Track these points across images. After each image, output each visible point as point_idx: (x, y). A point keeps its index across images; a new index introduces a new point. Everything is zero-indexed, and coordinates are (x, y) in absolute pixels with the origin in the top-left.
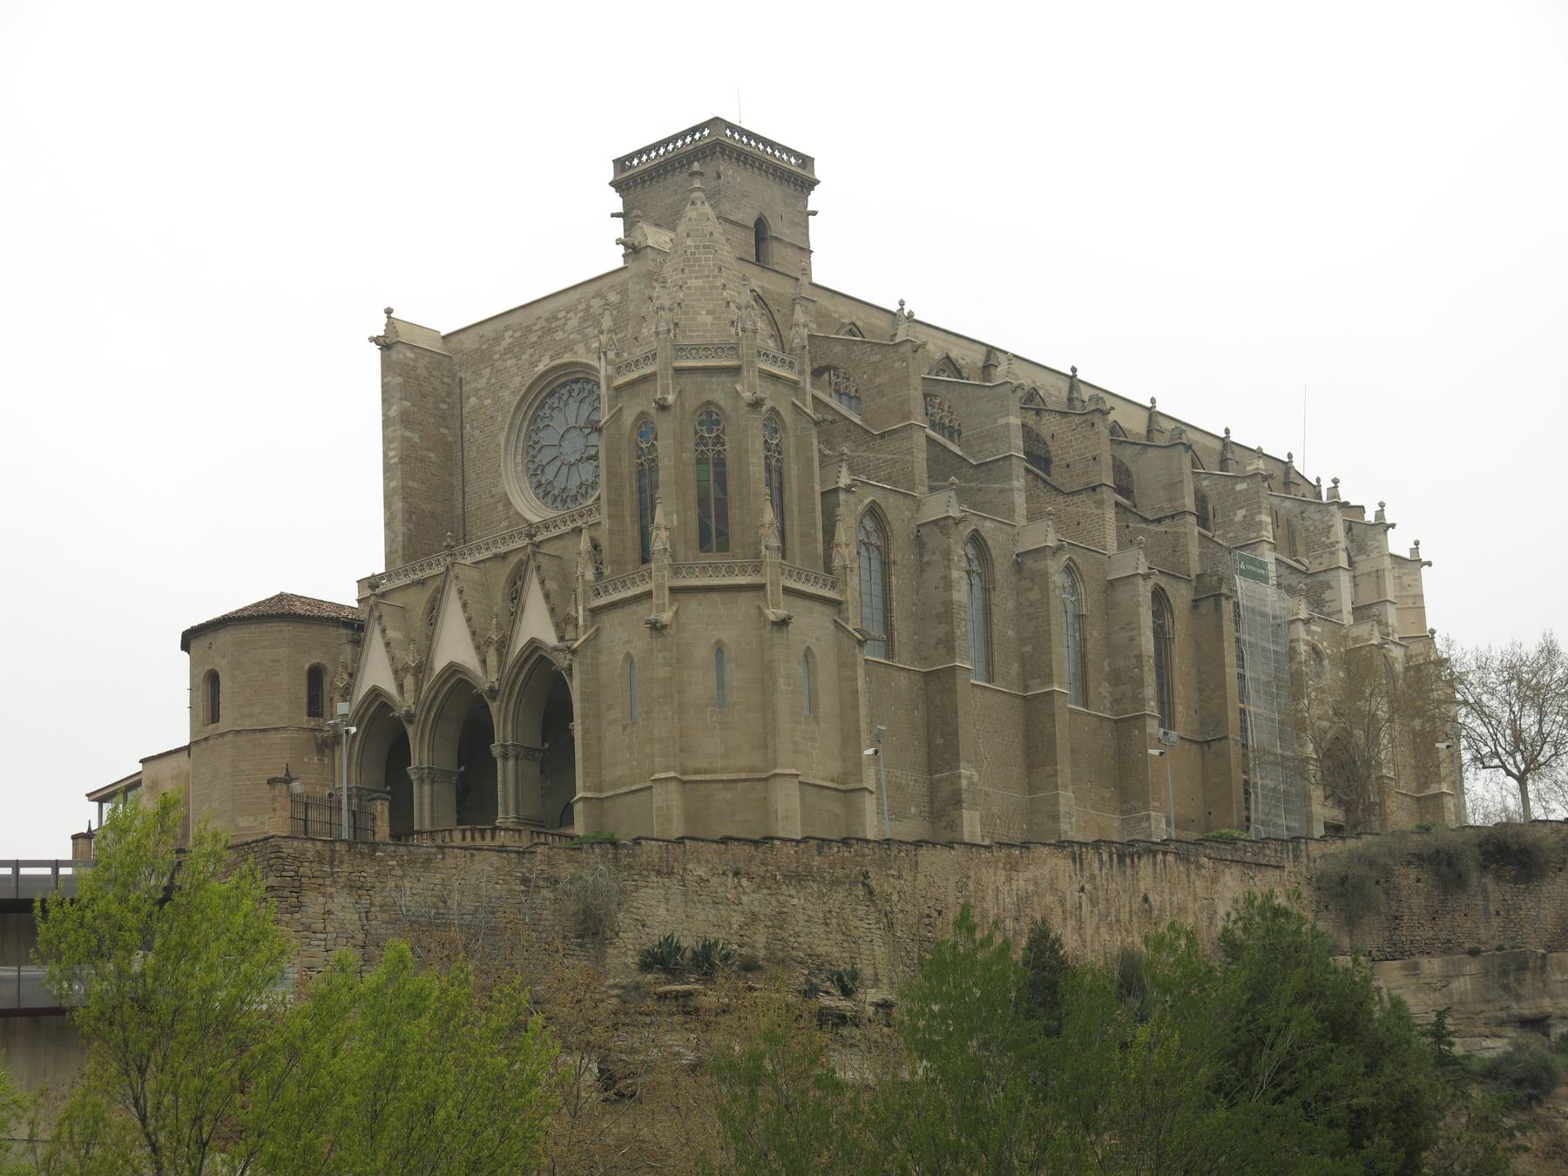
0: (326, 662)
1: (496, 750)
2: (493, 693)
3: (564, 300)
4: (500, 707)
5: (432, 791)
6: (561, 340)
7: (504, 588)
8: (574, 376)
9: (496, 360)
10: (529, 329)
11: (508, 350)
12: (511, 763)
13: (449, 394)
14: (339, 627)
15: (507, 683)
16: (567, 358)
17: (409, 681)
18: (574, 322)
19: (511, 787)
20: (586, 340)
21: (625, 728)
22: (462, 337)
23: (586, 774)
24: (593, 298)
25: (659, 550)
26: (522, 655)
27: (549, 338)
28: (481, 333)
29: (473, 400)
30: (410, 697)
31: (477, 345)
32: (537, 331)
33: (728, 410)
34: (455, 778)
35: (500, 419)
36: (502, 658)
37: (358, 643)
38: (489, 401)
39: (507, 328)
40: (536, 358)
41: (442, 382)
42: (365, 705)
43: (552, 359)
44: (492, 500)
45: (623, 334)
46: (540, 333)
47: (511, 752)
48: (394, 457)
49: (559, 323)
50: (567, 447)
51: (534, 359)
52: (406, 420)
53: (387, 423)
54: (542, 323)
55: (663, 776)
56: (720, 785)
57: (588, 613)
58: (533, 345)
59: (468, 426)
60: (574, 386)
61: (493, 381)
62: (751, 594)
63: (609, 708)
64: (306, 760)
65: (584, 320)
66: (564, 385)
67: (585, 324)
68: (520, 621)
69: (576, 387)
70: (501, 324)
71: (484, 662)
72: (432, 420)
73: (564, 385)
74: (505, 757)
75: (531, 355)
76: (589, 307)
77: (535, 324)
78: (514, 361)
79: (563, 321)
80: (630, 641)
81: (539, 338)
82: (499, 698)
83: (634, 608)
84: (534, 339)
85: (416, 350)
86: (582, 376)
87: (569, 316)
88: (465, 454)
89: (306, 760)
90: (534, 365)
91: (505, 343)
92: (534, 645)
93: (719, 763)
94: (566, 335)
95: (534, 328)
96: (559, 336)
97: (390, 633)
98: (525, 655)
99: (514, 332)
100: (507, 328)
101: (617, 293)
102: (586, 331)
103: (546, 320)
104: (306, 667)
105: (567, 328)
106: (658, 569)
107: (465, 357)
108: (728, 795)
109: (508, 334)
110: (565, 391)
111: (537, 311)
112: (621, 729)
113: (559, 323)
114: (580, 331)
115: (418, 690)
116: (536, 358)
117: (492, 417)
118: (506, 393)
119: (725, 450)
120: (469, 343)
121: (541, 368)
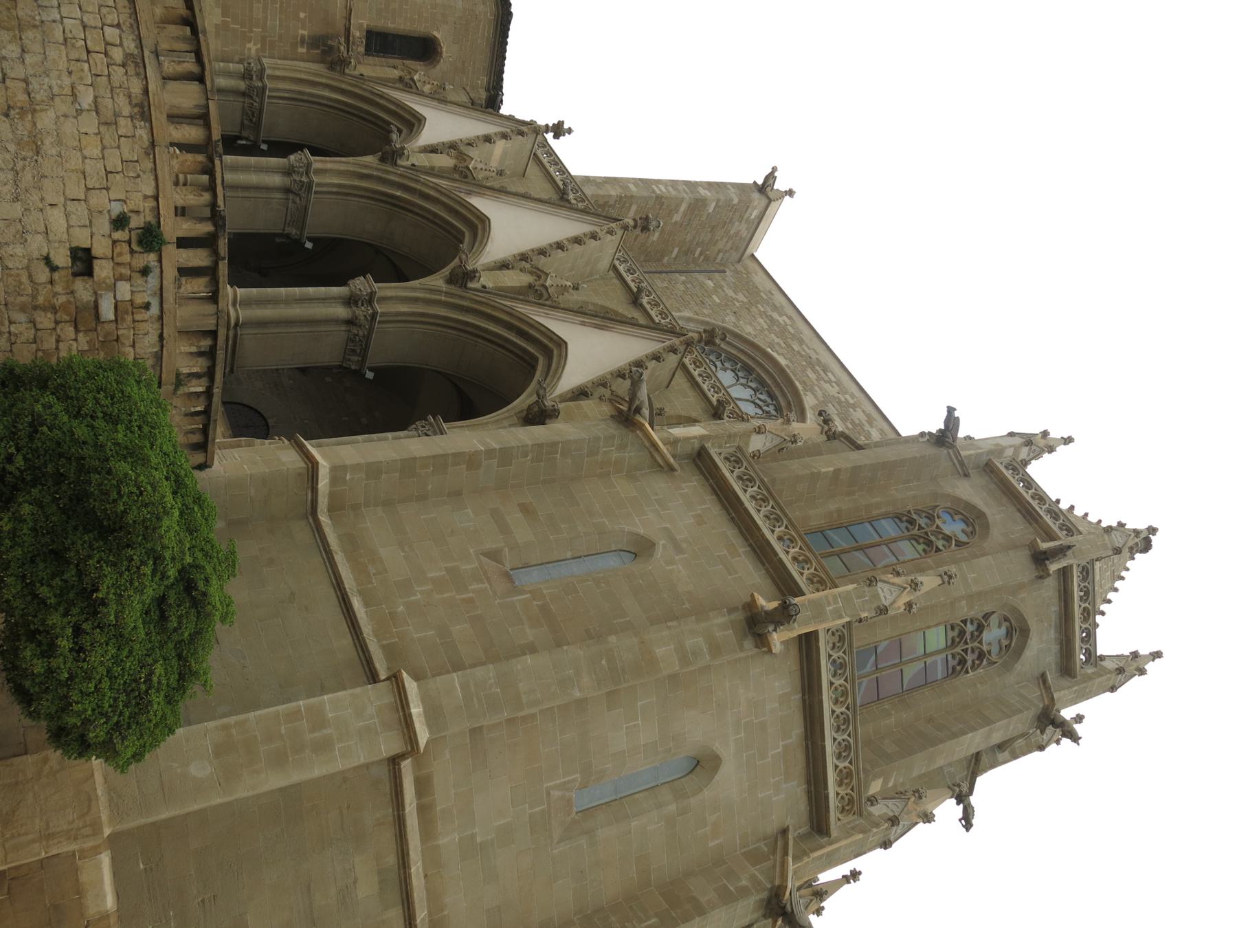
0: (443, 66)
1: (361, 284)
2: (462, 278)
3: (844, 377)
4: (439, 292)
5: (268, 189)
6: (807, 376)
7: (594, 304)
8: (778, 393)
10: (801, 342)
12: (341, 312)
13: (707, 259)
14: (488, 90)
15: (480, 303)
17: (444, 161)
19: (296, 311)
21: (494, 555)
22: (761, 273)
23: (373, 471)
24: (863, 411)
25: (876, 596)
26: (532, 326)
29: (710, 284)
30: (422, 160)
31: (762, 289)
32: (804, 350)
33: (1018, 666)
34: (293, 231)
36: (520, 294)
37: (473, 105)
39: (790, 318)
41: (719, 251)
42: (393, 107)
43: (787, 365)
46: (803, 353)
47: (361, 312)
48: (660, 190)
49: (822, 373)
51: (777, 348)
52: (698, 204)
53: (691, 185)
54: (814, 356)
55: (416, 710)
56: (391, 860)
57: (697, 445)
58: (789, 346)
61: (736, 303)
62: (803, 806)
63: (526, 510)
64: (302, 15)
68: (583, 324)
70: (790, 311)
71: (504, 266)
72: (689, 238)
74: (351, 301)
75: (778, 344)
76: (854, 406)
77: (809, 348)
79: (826, 378)
80: (678, 549)
81: (798, 352)
82: (454, 289)
83: (742, 548)
84: (796, 347)
85: (757, 221)
86: (783, 403)
87: (834, 384)
89: (302, 15)
92: (554, 349)
93: (448, 839)
95: (804, 346)
96: (812, 376)
97: (500, 145)
98: (532, 332)
99: (791, 326)
100: (790, 318)
104: (435, 33)
106: (847, 598)
107: (745, 276)
108: (367, 888)
109: (785, 318)
111: (821, 349)
112: (490, 545)
115: (431, 171)
119: (967, 672)
120: (758, 279)
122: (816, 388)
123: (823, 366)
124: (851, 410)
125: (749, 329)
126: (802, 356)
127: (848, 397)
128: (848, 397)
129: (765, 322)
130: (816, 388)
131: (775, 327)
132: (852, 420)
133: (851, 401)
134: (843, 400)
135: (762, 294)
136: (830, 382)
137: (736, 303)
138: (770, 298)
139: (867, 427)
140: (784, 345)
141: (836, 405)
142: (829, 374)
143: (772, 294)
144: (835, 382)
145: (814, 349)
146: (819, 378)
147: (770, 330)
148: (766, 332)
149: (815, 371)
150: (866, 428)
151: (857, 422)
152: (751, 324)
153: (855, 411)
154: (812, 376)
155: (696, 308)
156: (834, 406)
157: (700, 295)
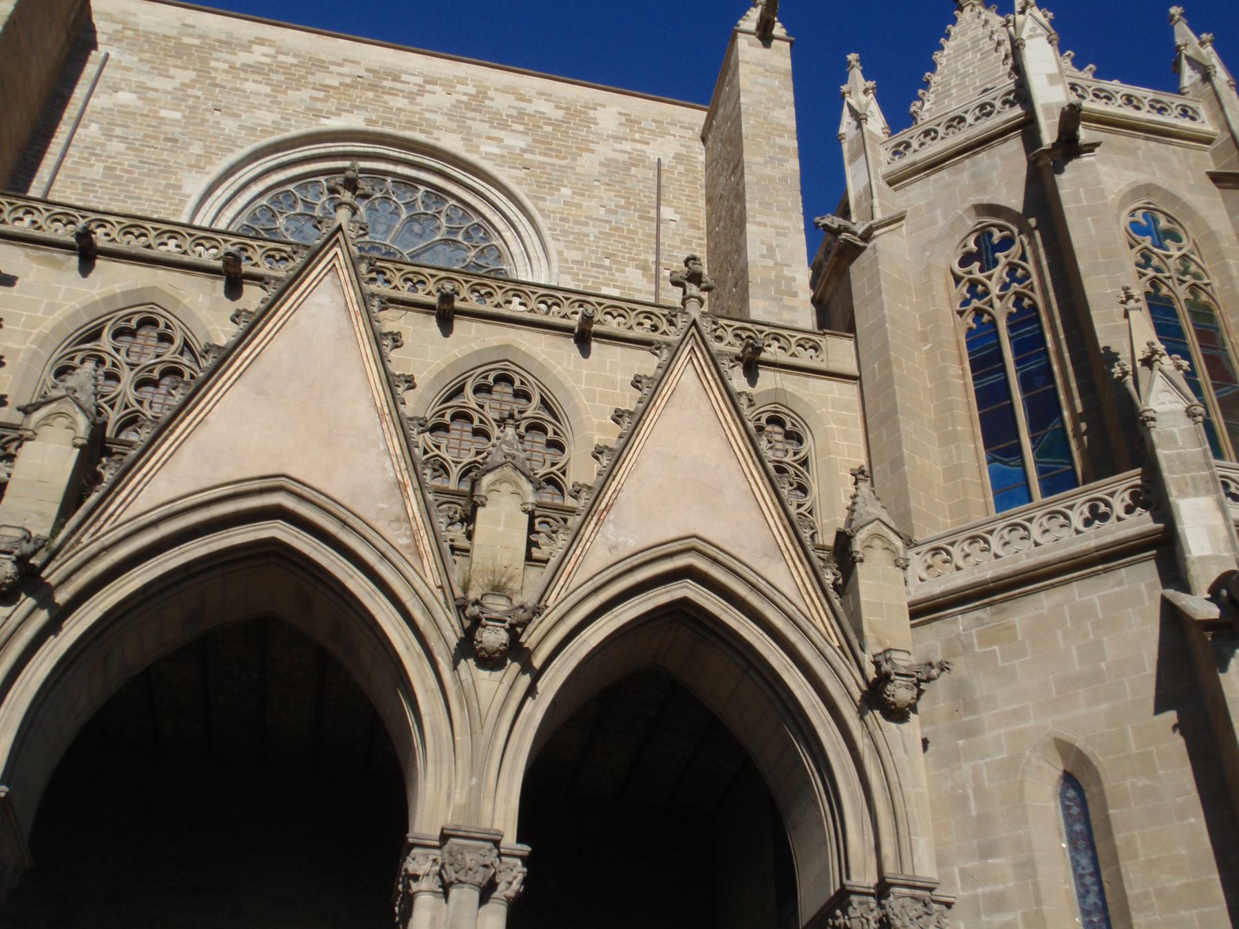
6: (399, 109)
9: (216, 69)
24: (496, 90)
27: (370, 95)
28: (189, 21)
31: (173, 33)
35: (196, 149)
38: (177, 115)
39: (261, 41)
45: (564, 163)
46: (348, 80)
51: (319, 105)
58: (325, 88)
59: (94, 127)
67: (469, 114)
75: (313, 99)
77: (341, 65)
78: (268, 89)
79: (415, 89)
81: (341, 84)
84: (334, 82)
87: (428, 87)
88: (68, 162)
90: (318, 114)
95: (332, 68)
96: (400, 102)
99: (279, 52)
100: (261, 41)
101: (558, 107)
102: (469, 123)
103: (367, 70)
105: (419, 99)
107: (129, 33)
117: (174, 141)
122: (427, 115)
123: (388, 74)
124: (487, 102)
125: (267, 117)
126: (352, 86)
127: (460, 88)
129: (255, 81)
130: (427, 115)
131: (275, 77)
132: (508, 116)
133: (473, 91)
134: (465, 98)
135: (186, 40)
136: (421, 92)
137: (190, 91)
138: (200, 37)
139: (530, 108)
140: (321, 95)
141: (473, 115)
142: (404, 77)
143: (193, 27)
144: (425, 82)
145: (345, 60)
146: (411, 97)
148: (281, 97)
149: (392, 92)
150: (532, 113)
151: (515, 113)
152: (253, 107)
153: (492, 99)
154: (400, 102)
155: (182, 159)
156: (474, 120)
157: (150, 131)
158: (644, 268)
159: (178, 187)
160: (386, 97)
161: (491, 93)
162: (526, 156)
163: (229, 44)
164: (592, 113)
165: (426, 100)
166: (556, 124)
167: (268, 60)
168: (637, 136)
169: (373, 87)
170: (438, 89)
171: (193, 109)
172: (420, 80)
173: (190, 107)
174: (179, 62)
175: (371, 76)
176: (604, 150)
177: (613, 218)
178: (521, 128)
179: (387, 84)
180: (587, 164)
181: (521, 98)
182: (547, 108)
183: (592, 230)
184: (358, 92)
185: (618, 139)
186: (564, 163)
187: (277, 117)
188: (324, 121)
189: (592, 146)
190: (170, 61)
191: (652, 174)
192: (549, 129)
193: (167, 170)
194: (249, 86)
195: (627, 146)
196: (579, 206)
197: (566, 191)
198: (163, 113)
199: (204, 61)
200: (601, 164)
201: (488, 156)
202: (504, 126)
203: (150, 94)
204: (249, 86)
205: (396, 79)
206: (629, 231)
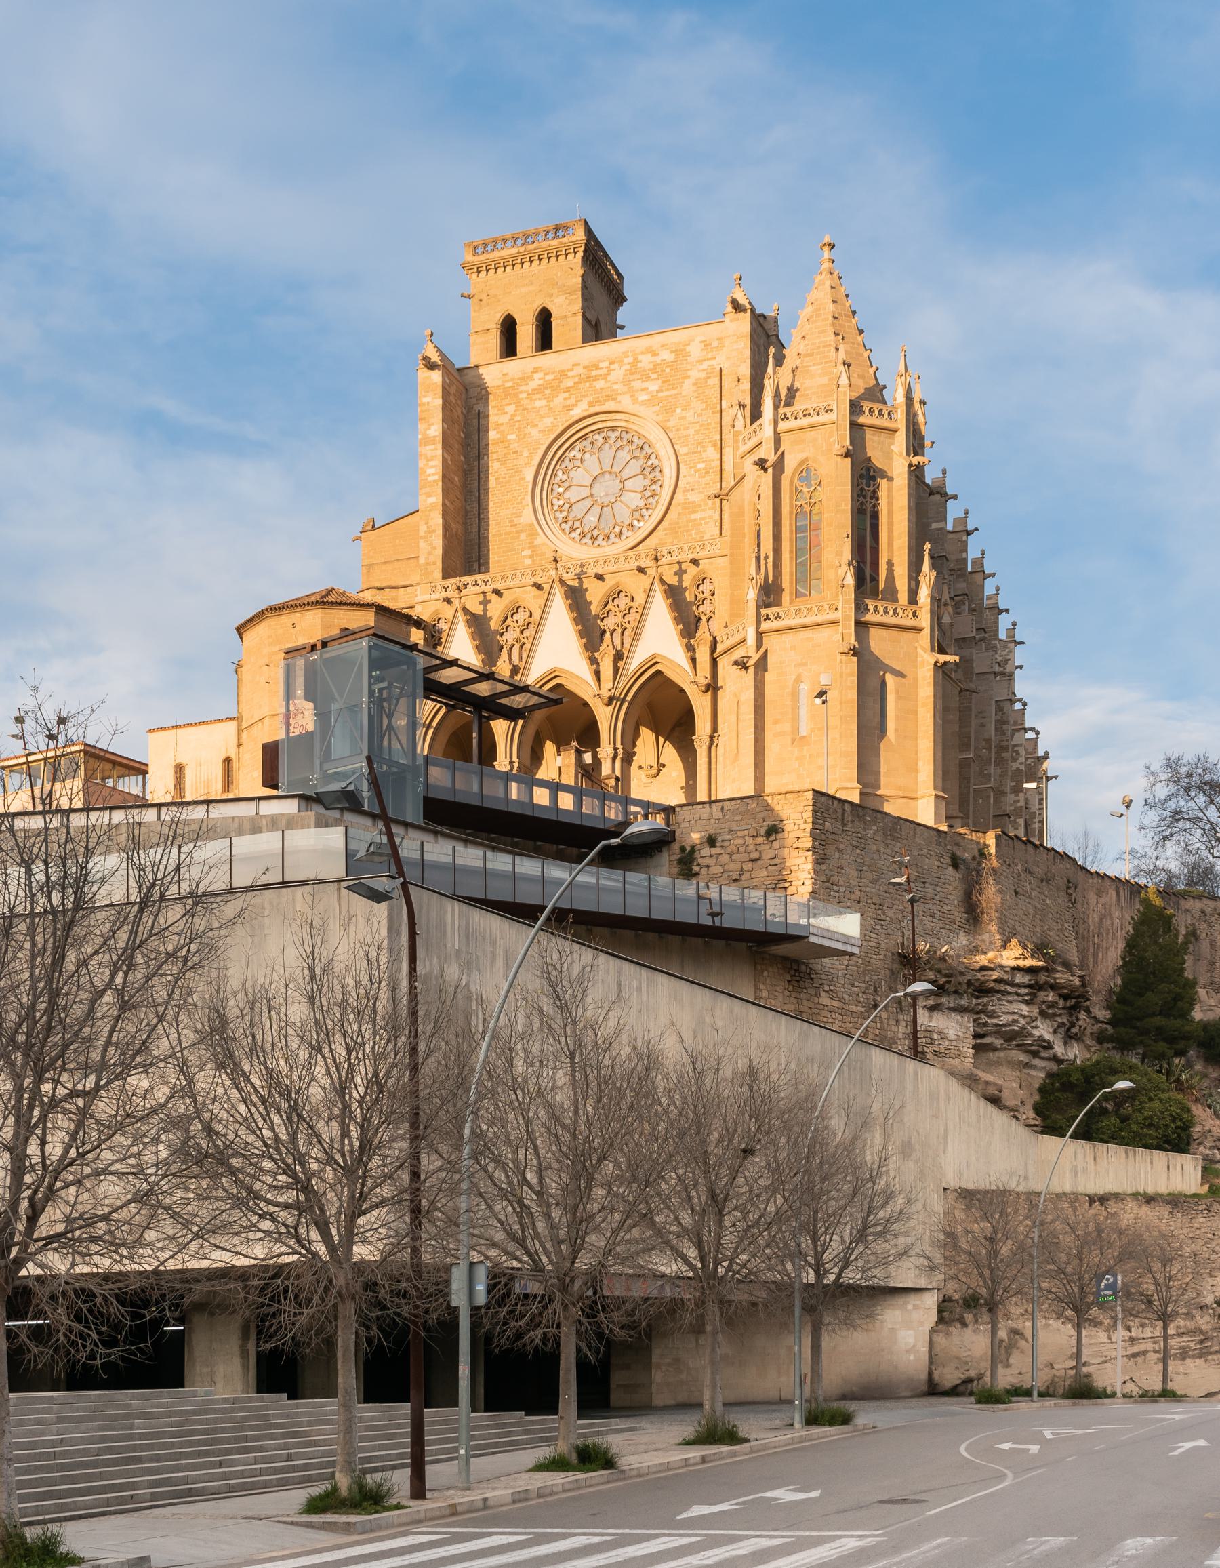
10: (563, 374)
11: (537, 391)
16: (610, 406)
18: (618, 373)
20: (633, 394)
31: (499, 383)
35: (526, 454)
39: (536, 370)
40: (572, 401)
43: (590, 404)
44: (514, 529)
46: (577, 379)
49: (599, 372)
50: (599, 490)
51: (568, 402)
58: (568, 389)
60: (610, 433)
65: (631, 372)
66: (598, 431)
67: (632, 377)
69: (613, 435)
73: (598, 431)
76: (636, 361)
77: (572, 370)
78: (544, 402)
79: (605, 371)
84: (570, 383)
87: (612, 367)
90: (569, 408)
91: (533, 385)
94: (608, 385)
95: (570, 374)
96: (600, 384)
99: (546, 374)
100: (536, 370)
102: (633, 384)
105: (609, 378)
109: (537, 376)
110: (599, 438)
113: (599, 372)
114: (626, 382)
116: (572, 401)
117: (516, 452)
118: (535, 432)
121: (577, 413)
122: (615, 387)
125: (548, 421)
127: (626, 360)
128: (626, 360)
130: (615, 387)
131: (547, 392)
133: (631, 359)
134: (628, 367)
138: (513, 379)
139: (658, 359)
140: (567, 395)
142: (601, 365)
147: (549, 399)
149: (596, 379)
151: (651, 366)
152: (542, 417)
158: (715, 446)
159: (523, 479)
160: (595, 383)
161: (641, 357)
162: (660, 394)
163: (525, 379)
164: (688, 349)
165: (611, 378)
166: (670, 365)
167: (541, 382)
168: (710, 356)
169: (589, 378)
170: (615, 366)
171: (519, 429)
172: (606, 364)
173: (519, 429)
174: (507, 401)
175: (585, 371)
176: (695, 374)
177: (700, 419)
178: (654, 376)
179: (594, 373)
180: (688, 386)
181: (655, 354)
182: (666, 356)
183: (691, 431)
184: (581, 386)
185: (701, 361)
186: (673, 392)
187: (551, 419)
188: (572, 413)
189: (689, 373)
190: (504, 402)
191: (717, 380)
192: (668, 370)
193: (518, 471)
194: (538, 404)
195: (705, 366)
196: (684, 418)
197: (679, 410)
198: (509, 437)
199: (516, 395)
200: (694, 384)
201: (643, 403)
202: (646, 378)
203: (502, 428)
204: (538, 404)
205: (597, 368)
206: (709, 424)
